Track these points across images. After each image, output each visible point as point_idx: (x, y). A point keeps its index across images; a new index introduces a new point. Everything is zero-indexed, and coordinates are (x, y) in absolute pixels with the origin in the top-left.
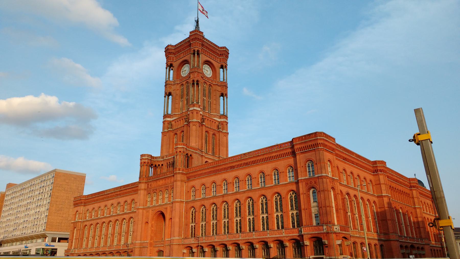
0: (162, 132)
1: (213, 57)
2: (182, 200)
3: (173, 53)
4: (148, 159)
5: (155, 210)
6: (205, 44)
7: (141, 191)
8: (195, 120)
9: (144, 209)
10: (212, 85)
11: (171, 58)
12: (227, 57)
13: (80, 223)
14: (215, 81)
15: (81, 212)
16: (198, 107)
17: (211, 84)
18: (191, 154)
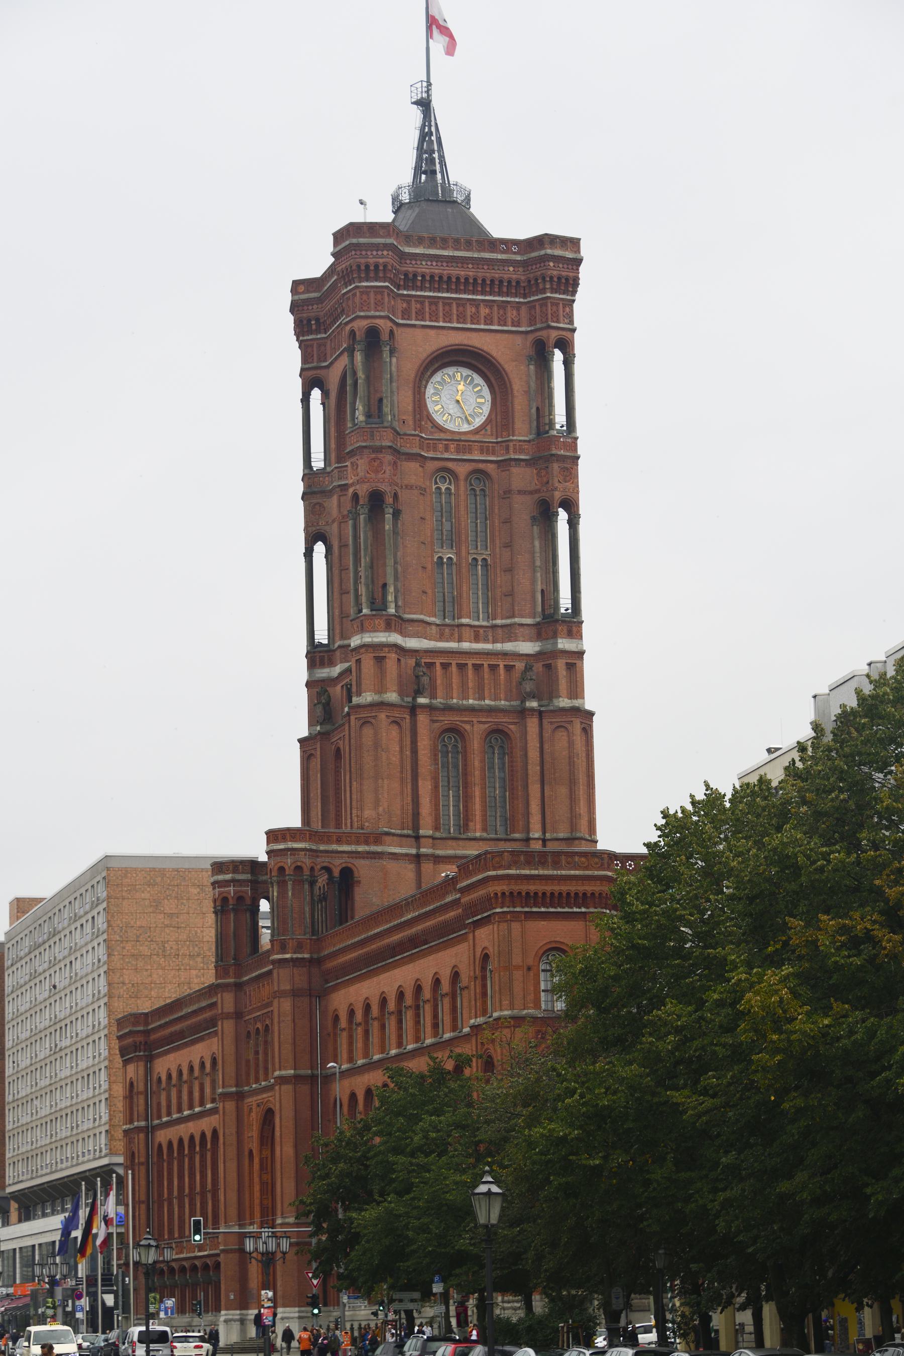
0: (300, 741)
1: (484, 311)
2: (302, 1072)
3: (317, 320)
4: (238, 881)
5: (262, 1103)
6: (424, 268)
7: (225, 1021)
8: (368, 697)
9: (239, 1097)
10: (490, 468)
11: (312, 346)
12: (571, 284)
13: (142, 1136)
14: (504, 444)
15: (141, 1088)
16: (383, 625)
17: (481, 466)
18: (344, 865)
